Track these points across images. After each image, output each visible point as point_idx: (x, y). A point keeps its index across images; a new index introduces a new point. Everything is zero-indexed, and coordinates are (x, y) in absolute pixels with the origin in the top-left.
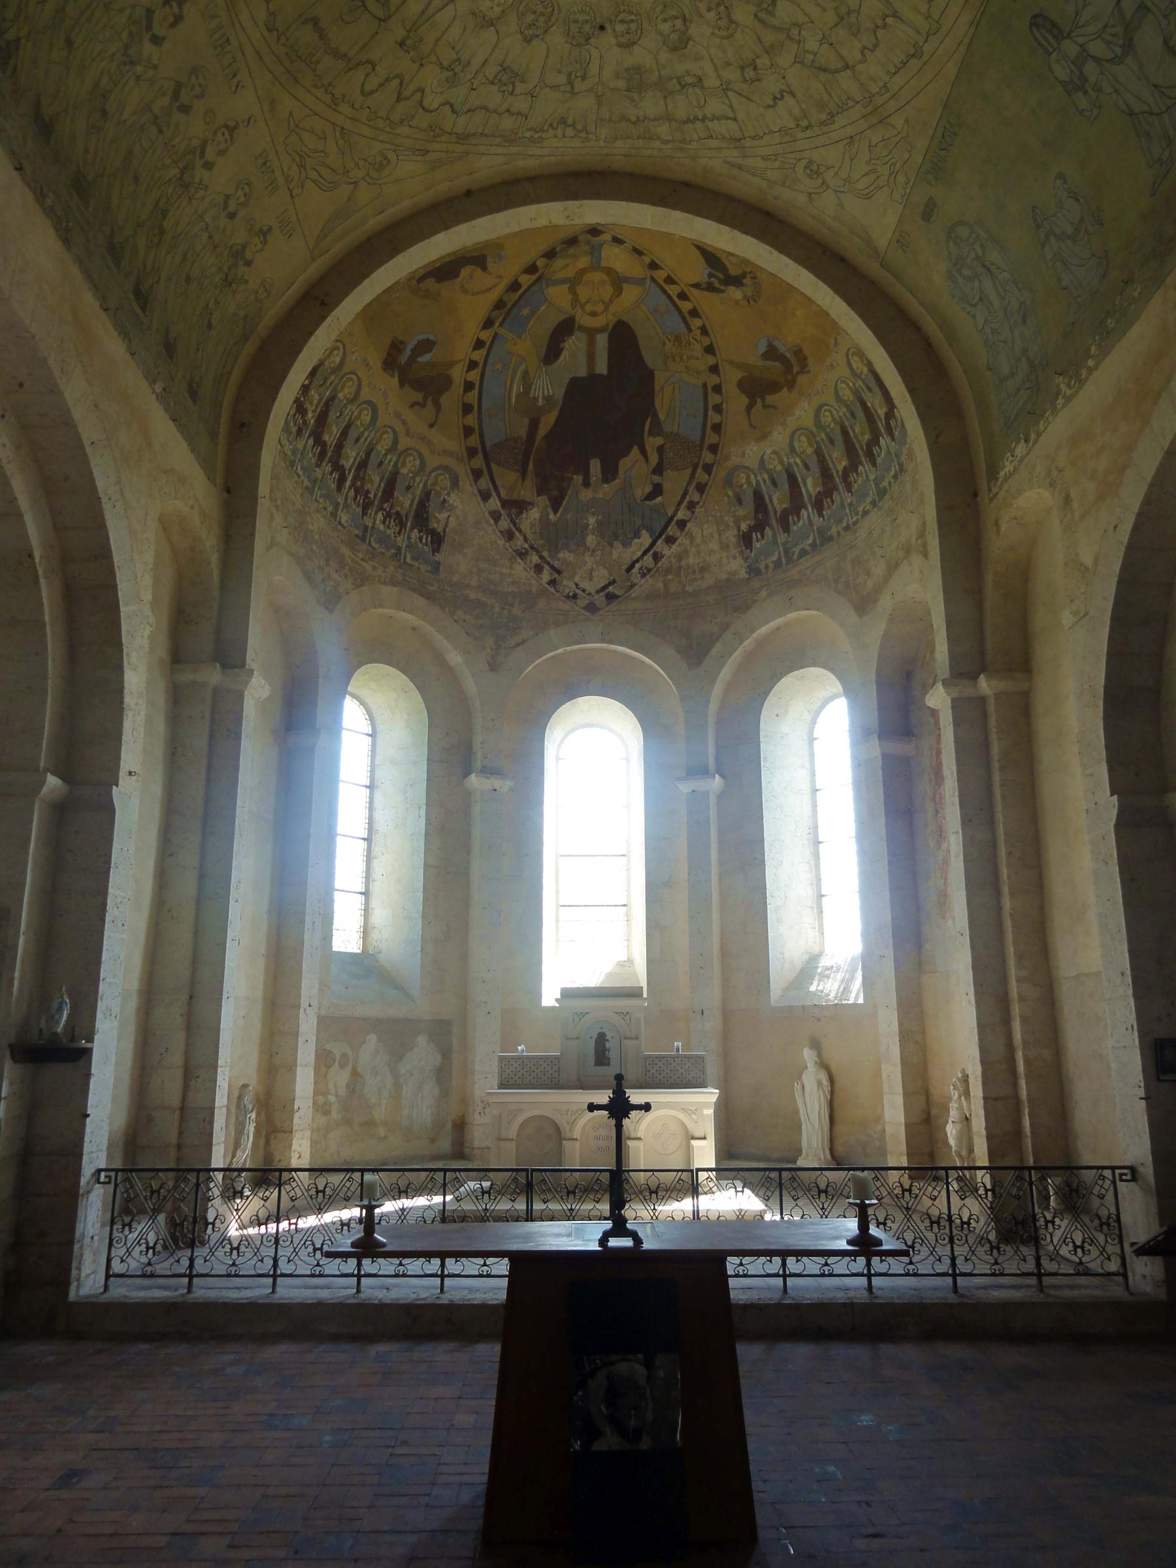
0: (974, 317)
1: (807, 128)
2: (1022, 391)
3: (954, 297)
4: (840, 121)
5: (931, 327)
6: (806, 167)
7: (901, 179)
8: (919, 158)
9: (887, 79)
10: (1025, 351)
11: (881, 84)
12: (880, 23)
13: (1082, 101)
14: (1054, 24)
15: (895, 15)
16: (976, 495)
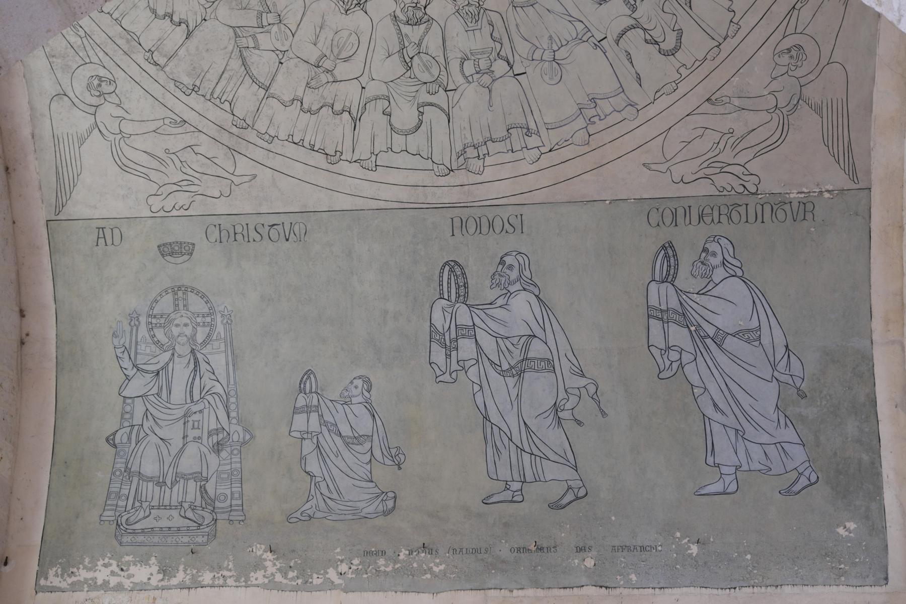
0: (128, 378)
1: (156, 64)
2: (175, 513)
3: (114, 335)
4: (194, 100)
5: (46, 330)
6: (100, 78)
7: (183, 199)
8: (221, 207)
9: (283, 136)
10: (201, 479)
11: (272, 132)
12: (338, 107)
13: (439, 355)
14: (466, 286)
15: (355, 121)
16: (6, 564)
